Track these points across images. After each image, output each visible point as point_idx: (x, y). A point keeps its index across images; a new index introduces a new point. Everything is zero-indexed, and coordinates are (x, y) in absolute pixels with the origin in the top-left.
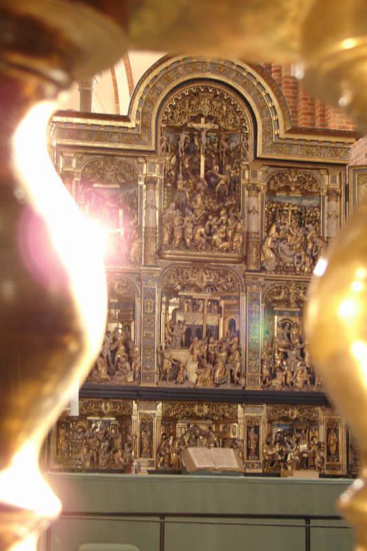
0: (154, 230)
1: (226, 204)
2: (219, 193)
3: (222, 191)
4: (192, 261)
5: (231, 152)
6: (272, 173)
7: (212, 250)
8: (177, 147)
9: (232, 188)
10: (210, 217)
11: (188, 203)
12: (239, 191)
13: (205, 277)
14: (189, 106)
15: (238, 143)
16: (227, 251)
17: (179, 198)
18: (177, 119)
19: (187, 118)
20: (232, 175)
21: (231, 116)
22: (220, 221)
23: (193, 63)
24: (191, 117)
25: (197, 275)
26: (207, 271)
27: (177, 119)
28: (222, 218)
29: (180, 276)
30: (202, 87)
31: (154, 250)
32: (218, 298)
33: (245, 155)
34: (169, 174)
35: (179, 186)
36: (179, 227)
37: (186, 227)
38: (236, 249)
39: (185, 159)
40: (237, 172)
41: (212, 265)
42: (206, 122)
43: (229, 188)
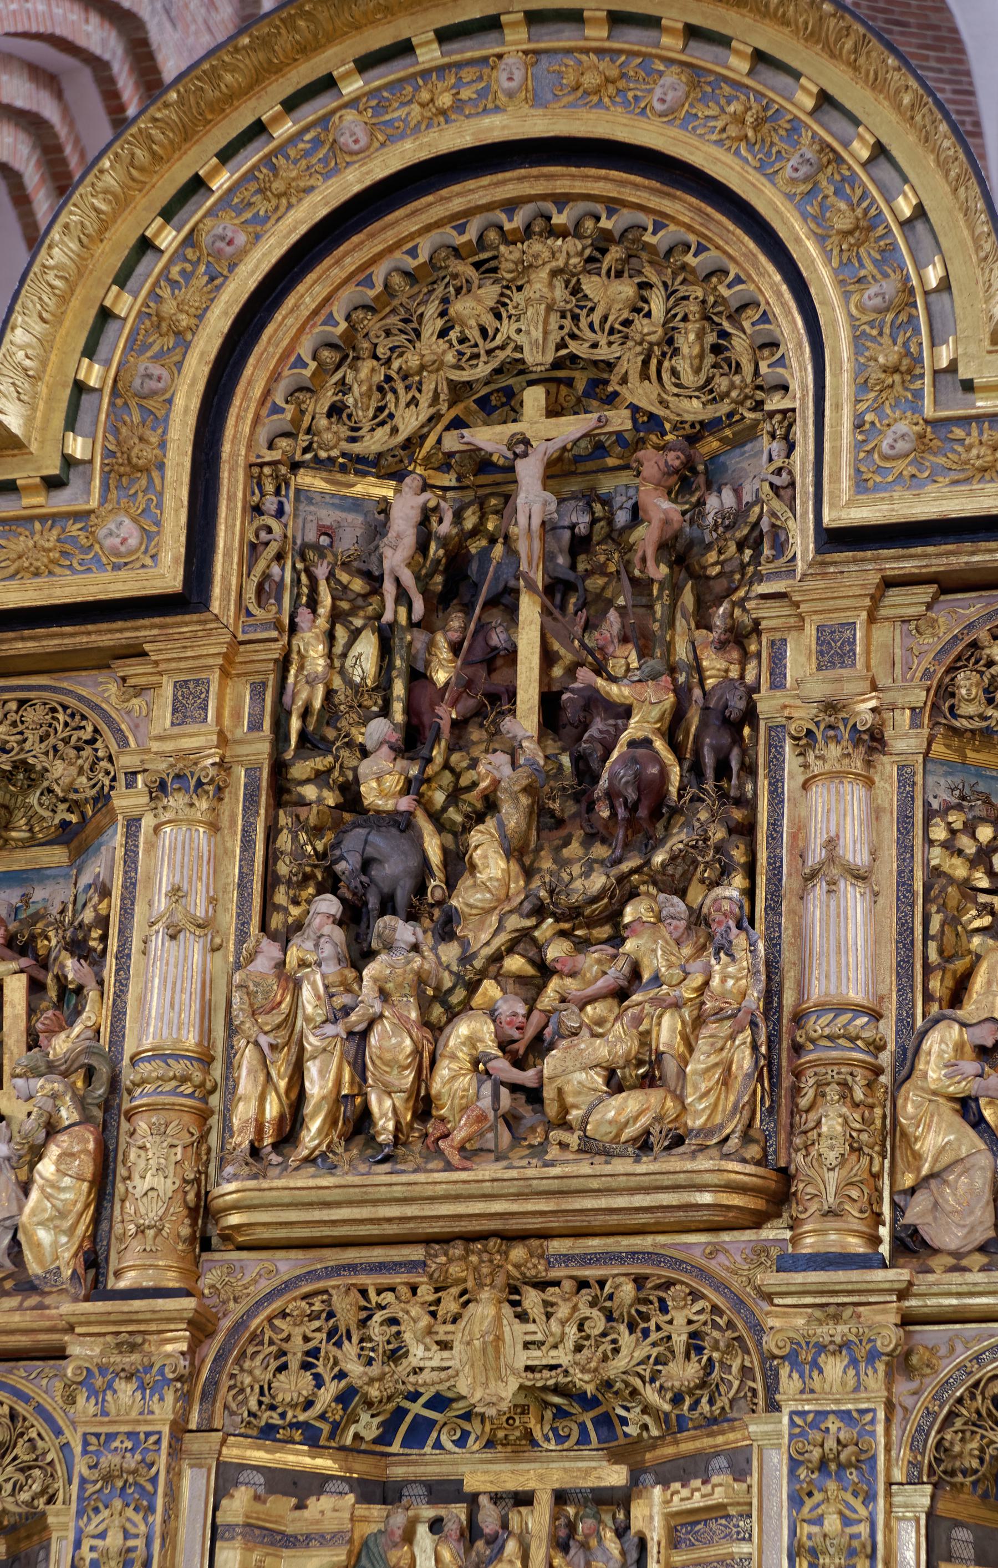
0: (178, 1068)
1: (659, 858)
2: (611, 795)
3: (639, 782)
4: (428, 1241)
5: (709, 547)
6: (970, 627)
7: (539, 1151)
8: (375, 581)
9: (709, 759)
10: (556, 951)
11: (435, 884)
12: (750, 770)
13: (515, 1331)
14: (443, 334)
15: (747, 497)
16: (643, 1145)
17: (367, 864)
18: (364, 416)
19: (424, 400)
20: (710, 682)
21: (688, 342)
22: (617, 972)
23: (426, 74)
24: (450, 382)
25: (457, 1334)
26: (532, 1299)
27: (364, 416)
28: (629, 946)
29: (350, 1349)
30: (510, 206)
31: (167, 1186)
32: (616, 1476)
33: (780, 546)
34: (330, 734)
35: (371, 793)
36: (330, 1029)
37: (373, 1021)
38: (706, 1131)
39: (430, 645)
40: (745, 657)
41: (567, 1259)
42: (554, 411)
43: (696, 769)
